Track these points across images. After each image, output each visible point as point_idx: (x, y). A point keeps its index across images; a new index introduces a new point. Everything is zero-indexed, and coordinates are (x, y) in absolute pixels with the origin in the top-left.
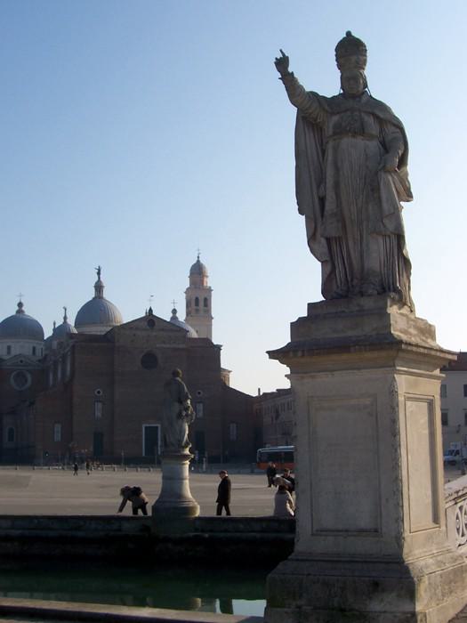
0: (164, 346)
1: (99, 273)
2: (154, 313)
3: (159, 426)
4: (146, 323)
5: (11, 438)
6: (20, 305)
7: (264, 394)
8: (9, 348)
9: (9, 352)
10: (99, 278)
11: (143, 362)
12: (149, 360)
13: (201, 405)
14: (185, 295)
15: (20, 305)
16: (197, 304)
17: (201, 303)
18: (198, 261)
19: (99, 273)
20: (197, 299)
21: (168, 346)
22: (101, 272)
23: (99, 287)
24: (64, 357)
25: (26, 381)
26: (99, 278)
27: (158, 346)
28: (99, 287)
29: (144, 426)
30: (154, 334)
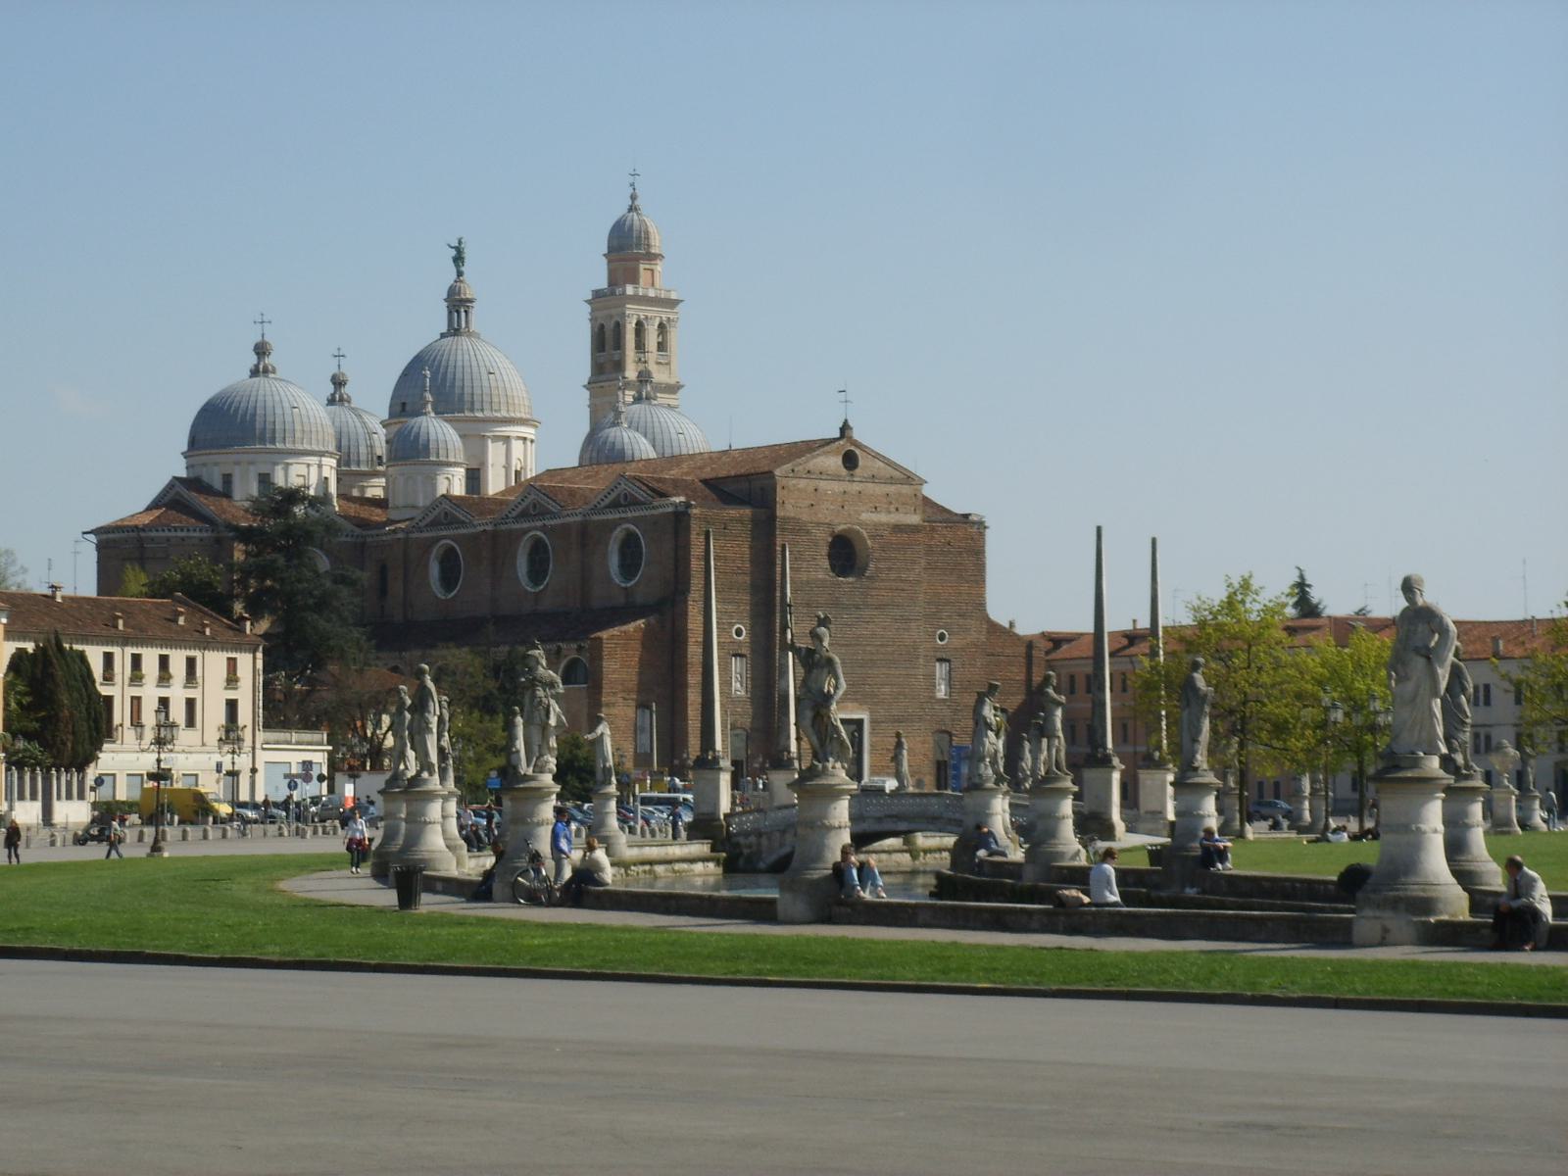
0: (876, 517)
1: (458, 259)
3: (865, 716)
4: (839, 460)
6: (261, 350)
10: (460, 274)
11: (830, 556)
12: (845, 553)
13: (945, 666)
14: (588, 308)
15: (261, 350)
16: (640, 346)
17: (652, 339)
18: (632, 209)
19: (458, 259)
20: (640, 328)
21: (883, 518)
22: (467, 255)
23: (457, 304)
26: (460, 274)
27: (865, 516)
28: (457, 304)
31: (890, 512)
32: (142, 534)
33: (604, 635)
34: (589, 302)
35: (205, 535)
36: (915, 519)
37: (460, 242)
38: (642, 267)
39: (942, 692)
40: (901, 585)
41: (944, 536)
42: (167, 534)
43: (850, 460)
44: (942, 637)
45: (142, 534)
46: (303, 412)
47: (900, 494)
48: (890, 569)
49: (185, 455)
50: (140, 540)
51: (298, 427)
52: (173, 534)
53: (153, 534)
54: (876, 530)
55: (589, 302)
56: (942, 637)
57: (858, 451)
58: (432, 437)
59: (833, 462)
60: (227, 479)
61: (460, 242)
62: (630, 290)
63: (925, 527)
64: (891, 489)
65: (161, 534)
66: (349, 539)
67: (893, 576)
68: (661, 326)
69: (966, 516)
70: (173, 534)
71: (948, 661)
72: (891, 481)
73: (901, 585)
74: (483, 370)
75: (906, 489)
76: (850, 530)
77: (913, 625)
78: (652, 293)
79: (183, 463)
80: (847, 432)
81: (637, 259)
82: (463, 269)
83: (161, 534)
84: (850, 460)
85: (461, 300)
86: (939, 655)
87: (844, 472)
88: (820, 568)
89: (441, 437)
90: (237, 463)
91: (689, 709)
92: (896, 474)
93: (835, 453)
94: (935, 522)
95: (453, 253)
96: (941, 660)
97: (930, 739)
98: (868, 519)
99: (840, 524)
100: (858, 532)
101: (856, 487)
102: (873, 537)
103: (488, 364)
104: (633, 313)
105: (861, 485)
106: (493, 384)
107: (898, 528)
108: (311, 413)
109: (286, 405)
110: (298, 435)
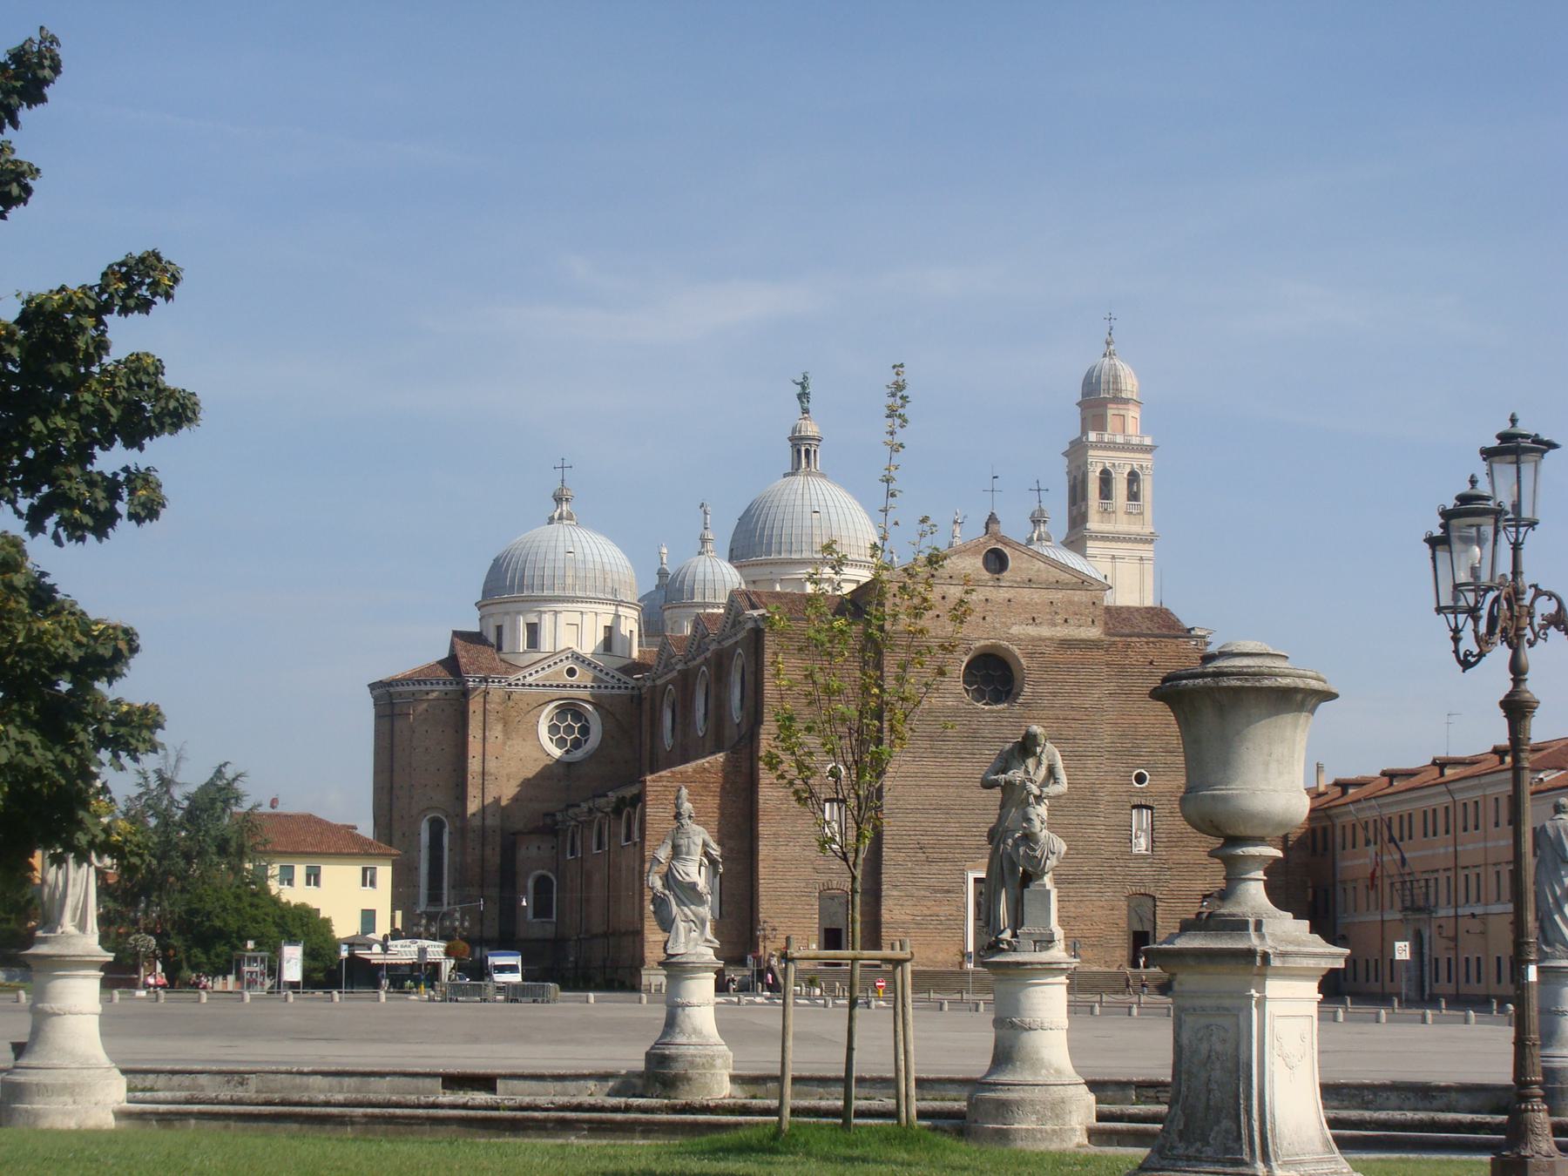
0: (1032, 631)
1: (803, 396)
2: (1004, 529)
5: (542, 909)
7: (1343, 785)
8: (533, 630)
9: (533, 642)
10: (806, 411)
12: (994, 674)
14: (1066, 461)
17: (1120, 488)
19: (803, 396)
20: (1106, 479)
21: (1045, 631)
22: (810, 390)
24: (720, 664)
25: (585, 731)
26: (806, 411)
27: (1015, 630)
29: (971, 876)
30: (1004, 594)
31: (1055, 625)
32: (392, 690)
33: (649, 778)
34: (1066, 454)
35: (449, 688)
36: (1094, 633)
37: (805, 378)
38: (1110, 412)
39: (1141, 845)
40: (1073, 714)
41: (1145, 654)
42: (412, 688)
43: (996, 561)
44: (1140, 779)
45: (392, 690)
46: (580, 557)
47: (1071, 602)
48: (1054, 694)
49: (480, 606)
50: (390, 695)
51: (570, 573)
52: (417, 688)
53: (400, 689)
54: (1034, 647)
55: (1066, 454)
56: (1140, 779)
57: (1007, 551)
58: (699, 577)
59: (973, 565)
60: (499, 629)
61: (805, 378)
62: (1093, 436)
63: (1114, 643)
64: (1058, 596)
65: (406, 688)
66: (622, 691)
67: (1059, 702)
68: (1133, 477)
69: (1189, 630)
70: (417, 688)
71: (1151, 808)
72: (1058, 585)
73: (1073, 714)
74: (807, 510)
75: (1079, 596)
76: (993, 646)
77: (1090, 763)
78: (1120, 439)
79: (477, 614)
80: (993, 527)
81: (1103, 403)
82: (810, 406)
83: (406, 688)
84: (996, 561)
85: (802, 438)
86: (1136, 801)
87: (986, 575)
88: (954, 692)
89: (709, 577)
90: (507, 613)
91: (761, 865)
92: (1065, 577)
93: (975, 553)
94: (1130, 636)
95: (798, 389)
96: (1139, 807)
97: (1123, 904)
98: (1016, 630)
99: (978, 639)
100: (1007, 649)
101: (1004, 594)
102: (1030, 655)
103: (815, 502)
104: (1097, 461)
105: (1012, 591)
106: (815, 523)
107: (1066, 644)
108: (589, 558)
109: (561, 550)
110: (569, 581)
